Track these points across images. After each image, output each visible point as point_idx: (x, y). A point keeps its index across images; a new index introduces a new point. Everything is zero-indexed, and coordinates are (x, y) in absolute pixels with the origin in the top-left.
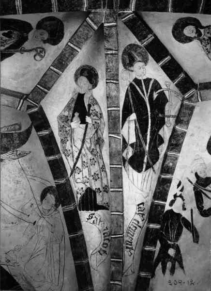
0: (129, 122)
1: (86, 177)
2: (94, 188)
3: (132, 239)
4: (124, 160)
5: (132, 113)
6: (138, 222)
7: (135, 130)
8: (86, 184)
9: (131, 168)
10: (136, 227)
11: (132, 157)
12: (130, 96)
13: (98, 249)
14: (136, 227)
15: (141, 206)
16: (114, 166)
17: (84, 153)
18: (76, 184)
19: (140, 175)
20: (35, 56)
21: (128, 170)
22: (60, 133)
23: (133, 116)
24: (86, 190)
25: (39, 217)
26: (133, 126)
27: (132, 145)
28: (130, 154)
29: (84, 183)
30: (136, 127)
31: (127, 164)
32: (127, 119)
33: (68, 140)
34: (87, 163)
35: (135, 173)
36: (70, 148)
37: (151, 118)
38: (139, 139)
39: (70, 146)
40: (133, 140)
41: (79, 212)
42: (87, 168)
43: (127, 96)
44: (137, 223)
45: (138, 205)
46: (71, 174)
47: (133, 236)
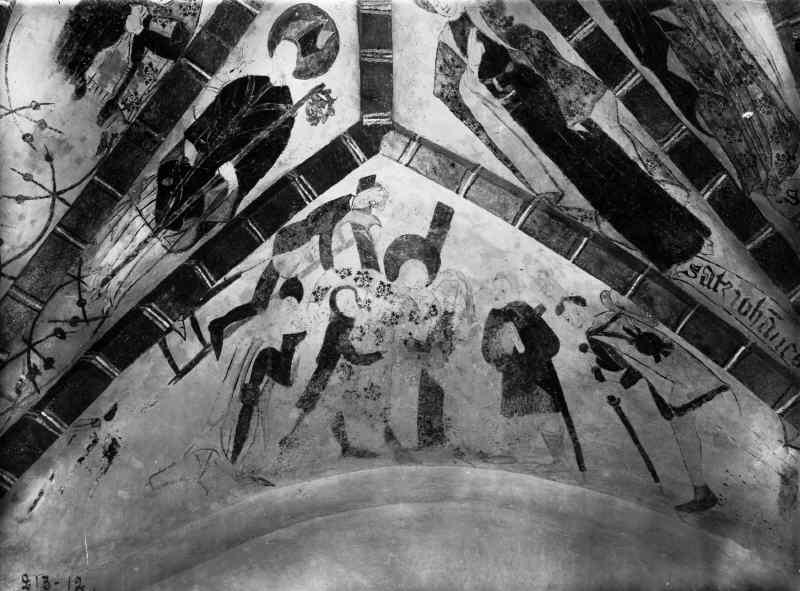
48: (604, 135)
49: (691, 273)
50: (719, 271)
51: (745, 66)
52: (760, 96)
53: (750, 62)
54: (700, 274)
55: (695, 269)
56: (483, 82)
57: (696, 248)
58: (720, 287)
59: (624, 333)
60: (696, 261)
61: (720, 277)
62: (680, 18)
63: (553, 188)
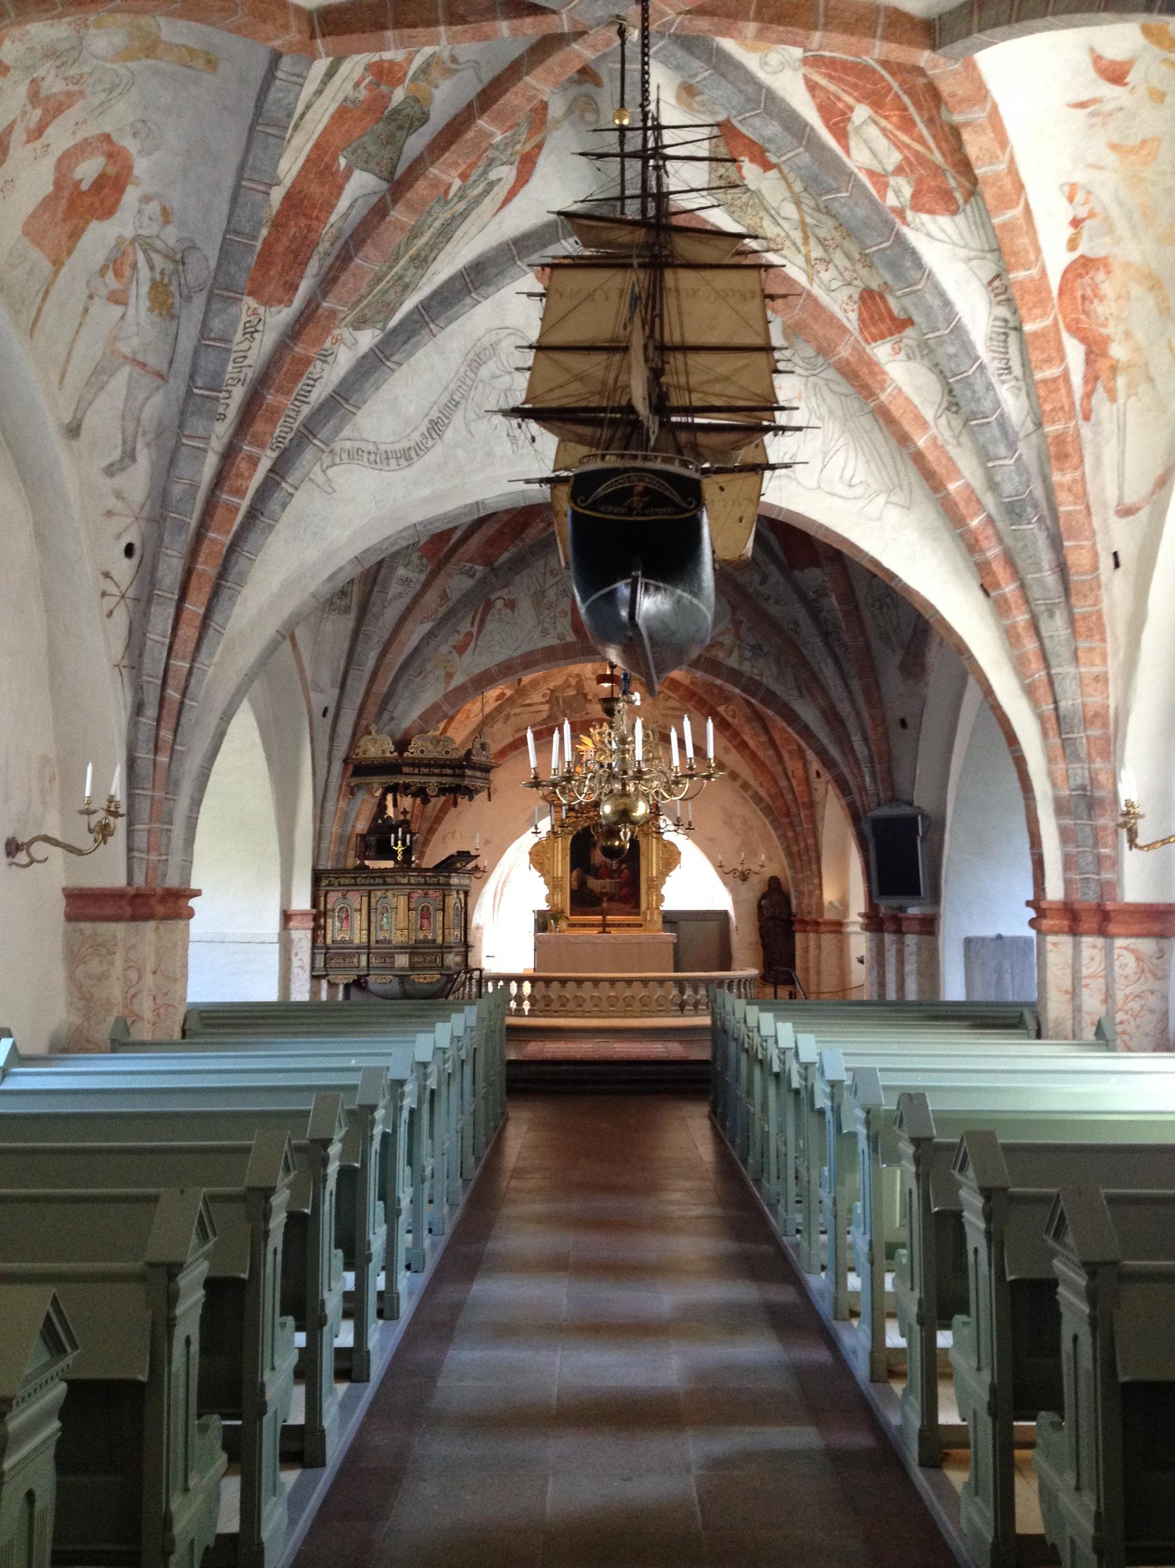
0: (858, 129)
1: (846, 269)
2: (874, 286)
3: (1008, 360)
4: (900, 212)
5: (852, 109)
6: (1005, 321)
7: (886, 136)
8: (856, 283)
9: (925, 217)
10: (1005, 334)
11: (914, 196)
12: (824, 82)
13: (945, 404)
14: (1005, 334)
15: (997, 283)
16: (874, 249)
17: (814, 222)
18: (833, 294)
19: (960, 218)
20: (582, 117)
21: (923, 224)
22: (735, 216)
23: (861, 113)
24: (862, 298)
25: (804, 379)
26: (873, 132)
27: (899, 170)
28: (907, 191)
29: (850, 284)
30: (883, 130)
31: (909, 214)
32: (850, 127)
33: (761, 219)
34: (833, 239)
35: (944, 221)
36: (777, 230)
37: (905, 92)
38: (908, 147)
39: (772, 226)
40: (893, 158)
41: (868, 349)
42: (838, 251)
43: (812, 87)
44: (1002, 324)
45: (990, 283)
46: (811, 280)
47: (1006, 353)
48: (341, 188)
49: (250, 312)
50: (260, 327)
51: (426, 258)
52: (407, 280)
53: (430, 259)
54: (252, 318)
55: (255, 312)
56: (365, 69)
57: (267, 303)
58: (248, 336)
59: (158, 270)
60: (261, 310)
61: (257, 331)
62: (455, 195)
63: (282, 177)
